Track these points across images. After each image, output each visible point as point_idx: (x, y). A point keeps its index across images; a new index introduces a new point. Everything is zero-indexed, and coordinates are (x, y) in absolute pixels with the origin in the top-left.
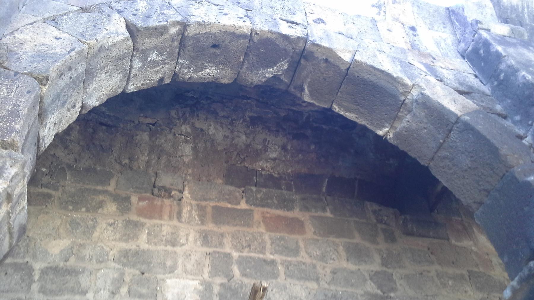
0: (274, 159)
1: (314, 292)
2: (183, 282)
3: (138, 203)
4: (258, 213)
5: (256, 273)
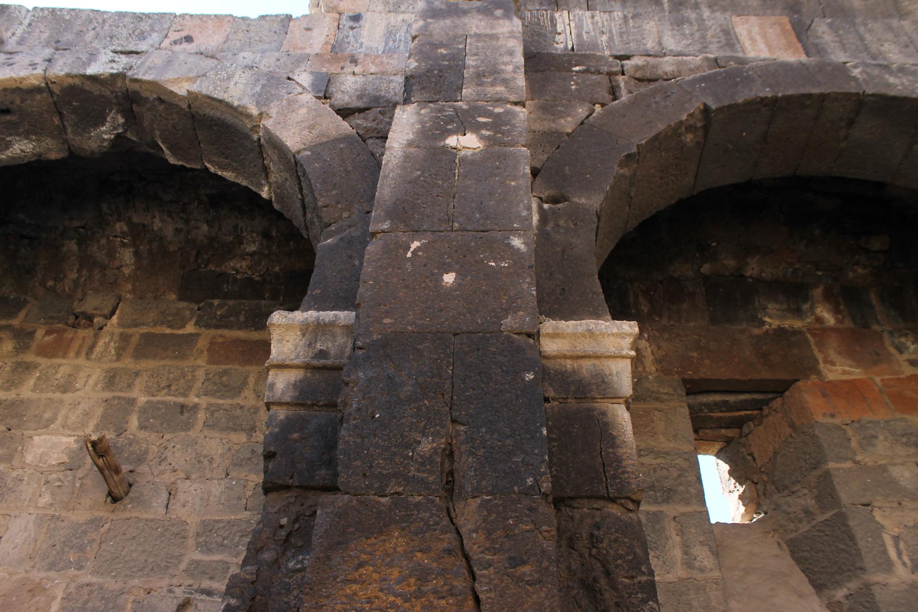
0: (252, 254)
1: (236, 447)
2: (54, 439)
3: (43, 337)
4: (206, 336)
5: (161, 424)
